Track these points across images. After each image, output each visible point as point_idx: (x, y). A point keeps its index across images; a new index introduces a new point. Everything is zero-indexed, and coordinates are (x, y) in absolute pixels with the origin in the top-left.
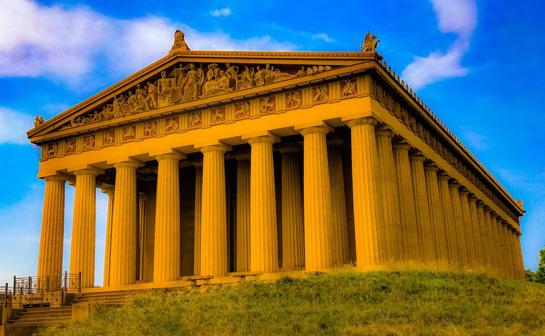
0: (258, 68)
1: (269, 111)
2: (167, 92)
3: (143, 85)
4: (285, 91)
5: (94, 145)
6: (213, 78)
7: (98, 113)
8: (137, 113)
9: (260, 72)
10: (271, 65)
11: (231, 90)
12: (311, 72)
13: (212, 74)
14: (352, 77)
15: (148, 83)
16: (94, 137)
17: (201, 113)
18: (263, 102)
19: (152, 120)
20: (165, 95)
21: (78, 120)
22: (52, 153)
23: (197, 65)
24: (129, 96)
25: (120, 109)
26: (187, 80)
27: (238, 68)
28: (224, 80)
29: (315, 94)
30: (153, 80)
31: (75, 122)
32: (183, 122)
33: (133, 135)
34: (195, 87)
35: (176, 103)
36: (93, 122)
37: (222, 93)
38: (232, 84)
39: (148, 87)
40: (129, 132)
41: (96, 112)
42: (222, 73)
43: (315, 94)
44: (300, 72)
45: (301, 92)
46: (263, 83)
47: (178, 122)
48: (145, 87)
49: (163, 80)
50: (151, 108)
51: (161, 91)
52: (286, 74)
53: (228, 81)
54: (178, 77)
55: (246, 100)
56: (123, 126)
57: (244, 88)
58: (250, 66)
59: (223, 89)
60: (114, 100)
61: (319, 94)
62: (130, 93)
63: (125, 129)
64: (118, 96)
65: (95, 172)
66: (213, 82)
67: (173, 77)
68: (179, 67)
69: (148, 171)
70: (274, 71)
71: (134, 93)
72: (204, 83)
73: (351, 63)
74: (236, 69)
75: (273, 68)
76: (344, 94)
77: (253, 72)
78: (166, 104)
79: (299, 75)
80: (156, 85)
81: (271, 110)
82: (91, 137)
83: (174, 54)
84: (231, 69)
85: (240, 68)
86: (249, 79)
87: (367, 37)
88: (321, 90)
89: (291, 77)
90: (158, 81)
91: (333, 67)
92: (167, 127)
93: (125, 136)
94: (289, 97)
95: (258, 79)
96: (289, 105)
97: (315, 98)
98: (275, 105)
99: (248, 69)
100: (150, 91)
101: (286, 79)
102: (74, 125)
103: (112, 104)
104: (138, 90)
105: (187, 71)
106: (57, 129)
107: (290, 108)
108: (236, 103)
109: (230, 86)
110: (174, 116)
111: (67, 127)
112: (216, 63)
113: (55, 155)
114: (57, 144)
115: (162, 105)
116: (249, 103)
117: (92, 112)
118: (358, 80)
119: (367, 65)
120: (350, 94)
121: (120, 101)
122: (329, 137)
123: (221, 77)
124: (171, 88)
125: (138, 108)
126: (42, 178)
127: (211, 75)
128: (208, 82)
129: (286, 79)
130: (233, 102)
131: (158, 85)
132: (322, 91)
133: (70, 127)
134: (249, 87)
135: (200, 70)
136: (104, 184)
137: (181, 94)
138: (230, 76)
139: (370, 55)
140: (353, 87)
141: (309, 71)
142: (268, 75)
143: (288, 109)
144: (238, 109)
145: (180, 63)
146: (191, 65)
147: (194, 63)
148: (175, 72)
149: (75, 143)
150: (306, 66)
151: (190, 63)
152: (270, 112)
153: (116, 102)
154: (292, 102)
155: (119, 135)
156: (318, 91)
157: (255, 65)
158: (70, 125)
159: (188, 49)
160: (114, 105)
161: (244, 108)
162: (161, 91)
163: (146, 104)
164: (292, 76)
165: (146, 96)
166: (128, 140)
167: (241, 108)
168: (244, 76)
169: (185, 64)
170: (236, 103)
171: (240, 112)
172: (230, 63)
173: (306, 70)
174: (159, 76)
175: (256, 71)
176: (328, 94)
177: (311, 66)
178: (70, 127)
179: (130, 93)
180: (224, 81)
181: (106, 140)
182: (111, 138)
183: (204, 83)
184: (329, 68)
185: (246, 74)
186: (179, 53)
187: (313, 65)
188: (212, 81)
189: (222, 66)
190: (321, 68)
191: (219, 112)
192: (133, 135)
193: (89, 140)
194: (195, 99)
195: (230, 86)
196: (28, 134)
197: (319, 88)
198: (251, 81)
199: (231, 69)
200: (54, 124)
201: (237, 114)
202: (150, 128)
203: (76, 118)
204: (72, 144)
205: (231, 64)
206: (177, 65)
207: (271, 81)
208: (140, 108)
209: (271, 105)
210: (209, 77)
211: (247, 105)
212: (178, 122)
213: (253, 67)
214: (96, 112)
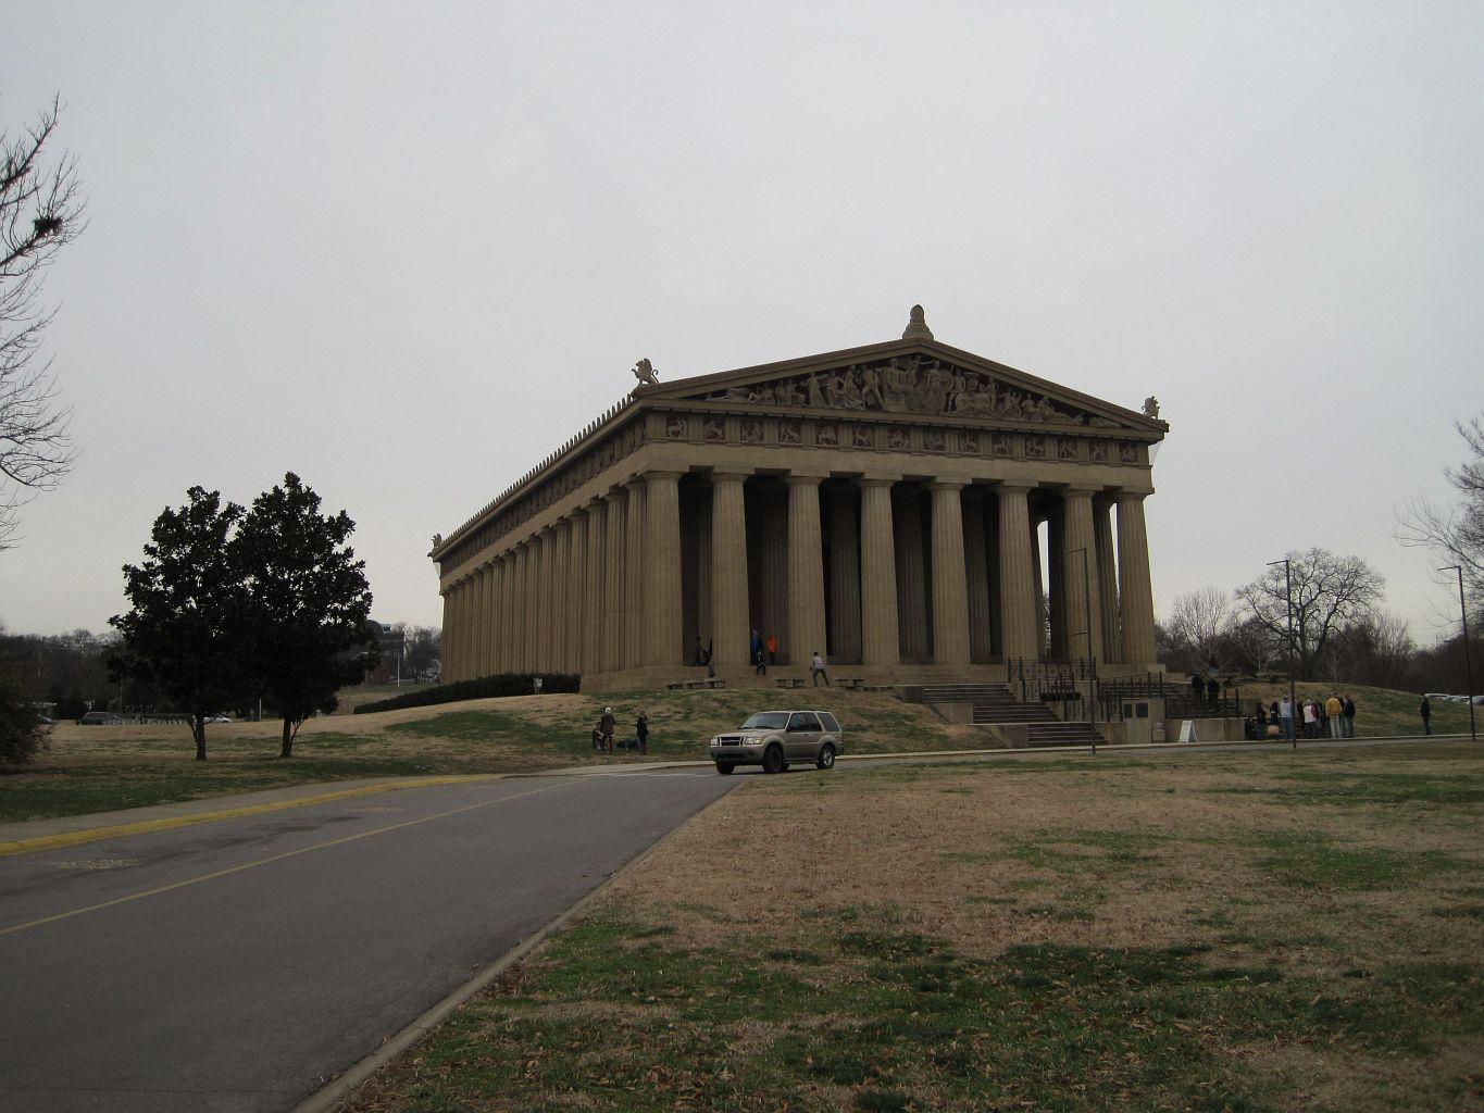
0: (1029, 396)
1: (1038, 456)
4: (1062, 438)
5: (761, 438)
8: (857, 410)
10: (1050, 399)
16: (761, 423)
23: (944, 366)
28: (984, 399)
32: (917, 439)
33: (835, 439)
37: (986, 416)
40: (830, 434)
44: (1078, 419)
47: (909, 438)
48: (858, 371)
49: (893, 369)
55: (1014, 434)
56: (822, 423)
64: (818, 374)
67: (905, 370)
73: (1140, 427)
82: (757, 426)
83: (918, 339)
84: (992, 386)
85: (1003, 387)
91: (1124, 426)
93: (821, 437)
97: (1094, 455)
104: (850, 373)
106: (702, 397)
108: (997, 435)
113: (680, 438)
117: (762, 385)
144: (996, 441)
145: (919, 353)
147: (942, 362)
149: (724, 426)
150: (1094, 415)
155: (808, 434)
166: (825, 445)
169: (925, 358)
170: (997, 435)
174: (885, 363)
176: (1106, 452)
177: (1098, 416)
182: (796, 435)
189: (984, 380)
191: (970, 440)
199: (992, 386)
205: (995, 380)
206: (913, 356)
209: (1039, 448)
210: (959, 385)
212: (909, 438)
213: (1023, 394)
214: (766, 386)
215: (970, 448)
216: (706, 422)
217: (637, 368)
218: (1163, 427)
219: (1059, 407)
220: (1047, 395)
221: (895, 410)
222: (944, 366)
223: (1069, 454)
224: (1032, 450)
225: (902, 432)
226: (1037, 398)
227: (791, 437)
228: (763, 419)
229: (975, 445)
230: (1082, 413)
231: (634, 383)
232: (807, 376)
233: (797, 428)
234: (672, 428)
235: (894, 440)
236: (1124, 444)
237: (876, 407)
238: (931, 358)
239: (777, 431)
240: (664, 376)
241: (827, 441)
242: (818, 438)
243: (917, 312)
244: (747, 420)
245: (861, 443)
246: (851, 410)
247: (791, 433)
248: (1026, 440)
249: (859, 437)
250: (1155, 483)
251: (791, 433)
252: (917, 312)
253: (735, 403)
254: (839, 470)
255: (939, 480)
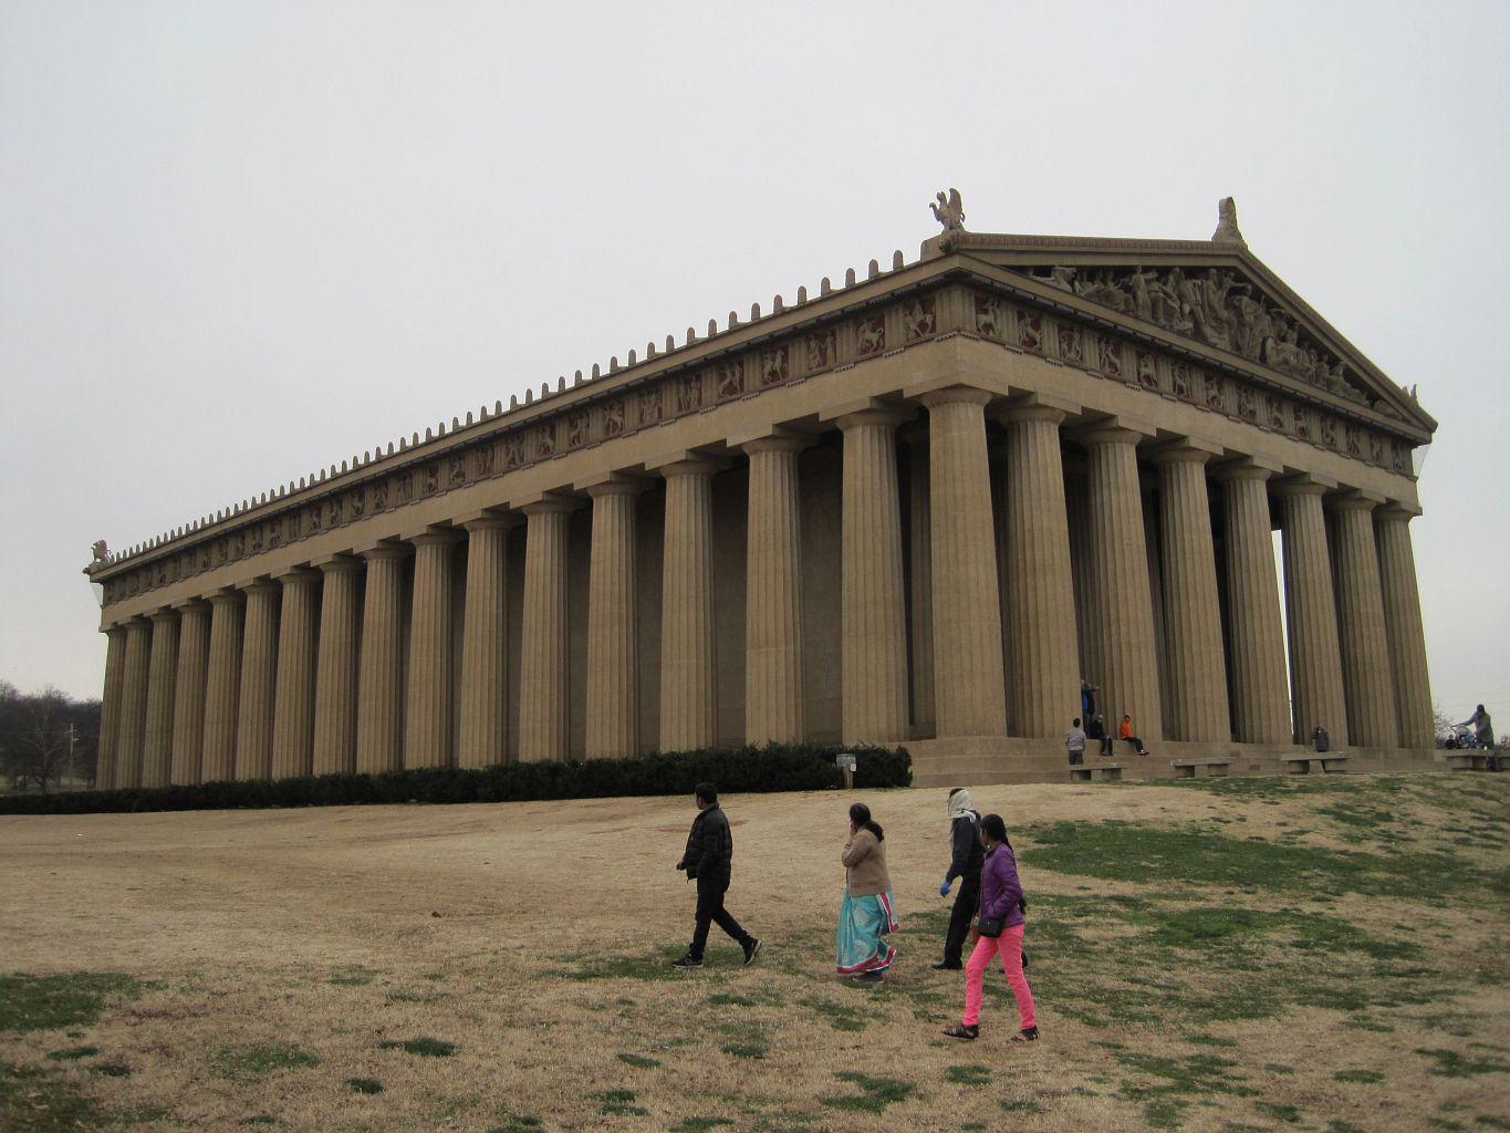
20: (1225, 325)
22: (988, 327)
23: (1257, 296)
37: (1299, 377)
60: (1135, 272)
64: (1146, 269)
73: (1414, 421)
91: (1405, 420)
158: (1053, 278)
169: (1240, 277)
170: (1303, 405)
177: (1385, 401)
193: (1071, 339)
213: (1322, 351)
217: (938, 204)
218: (1429, 426)
219: (1350, 376)
221: (1217, 348)
222: (1257, 296)
226: (1334, 362)
227: (1112, 365)
231: (938, 229)
232: (1130, 271)
234: (984, 319)
237: (1198, 335)
238: (1248, 281)
240: (976, 222)
242: (1139, 374)
243: (1228, 208)
244: (1072, 324)
245: (1181, 390)
247: (1113, 359)
248: (1322, 420)
250: (1423, 501)
251: (1113, 359)
252: (1228, 208)
255: (1257, 462)
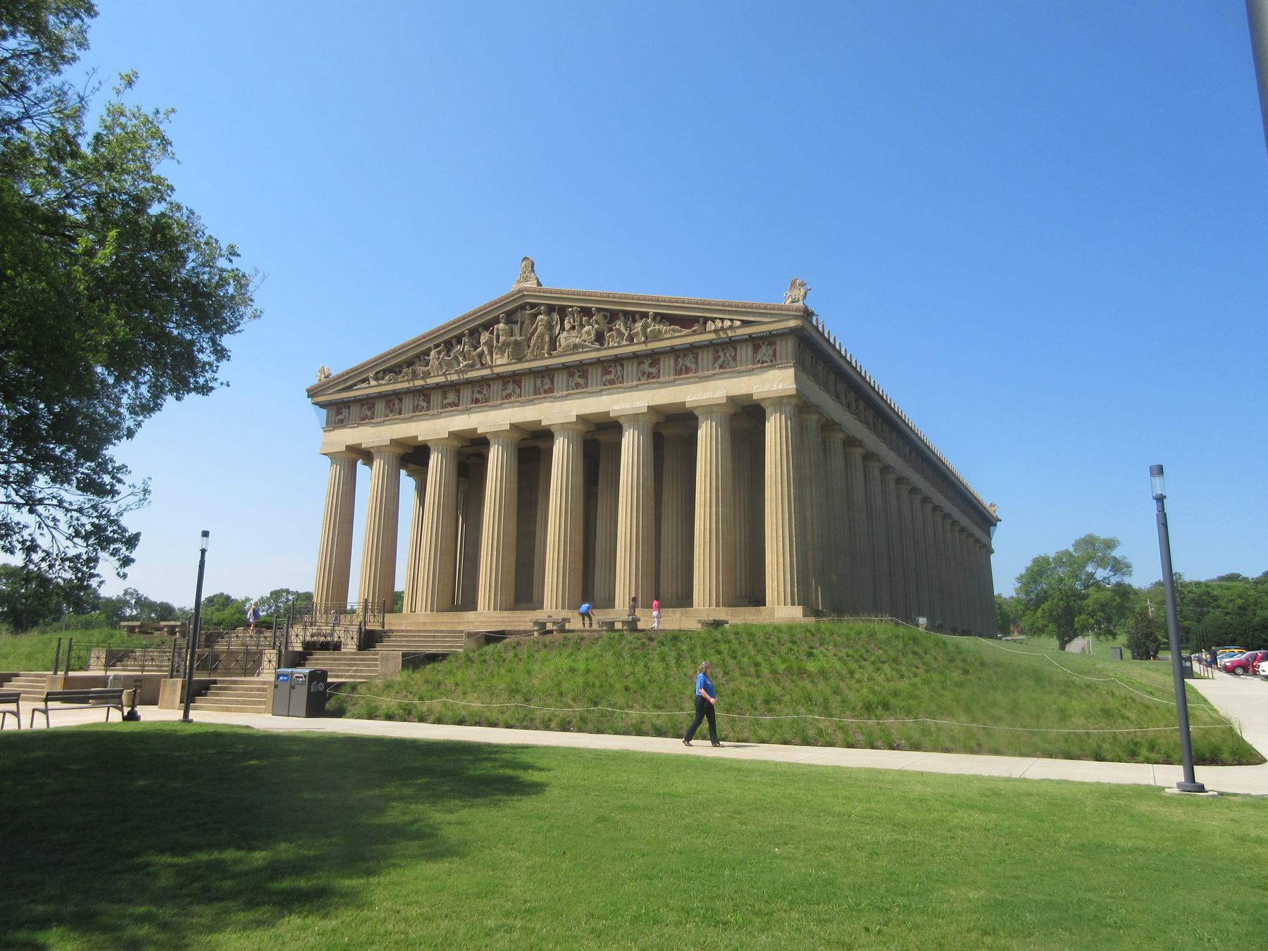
0: (637, 316)
2: (506, 345)
3: (474, 333)
4: (674, 352)
6: (573, 328)
7: (408, 367)
9: (639, 325)
10: (656, 314)
11: (597, 345)
12: (713, 327)
13: (572, 321)
14: (770, 339)
15: (480, 329)
16: (401, 400)
17: (553, 376)
18: (643, 365)
19: (483, 382)
21: (380, 375)
23: (550, 309)
24: (452, 346)
25: (440, 363)
26: (536, 329)
27: (608, 315)
29: (716, 359)
30: (487, 326)
31: (376, 379)
34: (547, 339)
35: (520, 360)
36: (400, 380)
38: (600, 338)
39: (480, 335)
40: (451, 397)
41: (404, 366)
42: (586, 321)
43: (716, 359)
45: (697, 354)
46: (643, 339)
47: (520, 387)
49: (501, 326)
50: (483, 366)
51: (498, 341)
52: (677, 327)
53: (593, 333)
54: (523, 323)
55: (619, 360)
57: (616, 345)
58: (626, 313)
59: (587, 343)
61: (722, 358)
62: (454, 342)
63: (445, 393)
64: (437, 346)
65: (399, 451)
66: (574, 333)
67: (516, 322)
68: (526, 310)
69: (474, 450)
70: (660, 322)
71: (459, 342)
72: (559, 334)
74: (605, 317)
75: (658, 318)
76: (758, 362)
77: (629, 323)
78: (505, 361)
79: (694, 331)
80: (492, 333)
81: (654, 378)
82: (396, 402)
83: (520, 291)
85: (612, 316)
86: (624, 331)
87: (793, 285)
88: (725, 354)
89: (683, 333)
90: (496, 326)
92: (504, 393)
94: (680, 360)
95: (637, 334)
96: (679, 372)
98: (659, 371)
99: (622, 318)
100: (482, 340)
101: (677, 334)
102: (373, 383)
103: (429, 355)
105: (535, 315)
106: (350, 388)
107: (681, 377)
109: (596, 340)
110: (514, 379)
111: (364, 385)
112: (579, 307)
114: (349, 408)
115: (499, 362)
116: (622, 366)
118: (778, 344)
119: (792, 323)
120: (767, 362)
121: (439, 353)
122: (733, 418)
123: (584, 326)
124: (513, 339)
125: (465, 363)
126: (326, 454)
127: (570, 322)
128: (565, 333)
129: (677, 334)
130: (598, 362)
131: (495, 333)
132: (728, 355)
133: (367, 385)
134: (624, 343)
135: (556, 316)
136: (410, 465)
137: (526, 348)
138: (596, 326)
139: (797, 310)
140: (771, 352)
141: (710, 326)
142: (652, 328)
143: (677, 377)
144: (606, 372)
146: (542, 308)
148: (518, 316)
150: (706, 320)
151: (541, 304)
152: (652, 380)
153: (432, 353)
154: (684, 368)
156: (721, 354)
157: (633, 314)
159: (539, 284)
160: (431, 357)
161: (615, 371)
162: (498, 341)
163: (477, 359)
164: (685, 331)
165: (476, 348)
167: (610, 373)
168: (617, 327)
169: (533, 306)
171: (608, 377)
172: (597, 308)
173: (705, 323)
175: (634, 321)
177: (713, 320)
178: (367, 385)
179: (454, 342)
180: (588, 333)
181: (417, 406)
182: (424, 404)
183: (559, 334)
184: (738, 323)
185: (619, 325)
186: (526, 289)
187: (716, 318)
188: (571, 332)
189: (586, 312)
190: (727, 323)
191: (580, 376)
192: (457, 401)
193: (394, 405)
194: (546, 355)
195: (596, 340)
196: (308, 391)
197: (723, 350)
198: (627, 334)
200: (345, 380)
201: (604, 379)
202: (480, 392)
203: (377, 373)
204: (369, 409)
205: (599, 310)
206: (523, 307)
207: (657, 336)
208: (468, 365)
209: (654, 370)
210: (567, 326)
211: (619, 368)
213: (631, 317)
214: (404, 366)
215: (578, 386)
216: (363, 405)
220: (652, 311)
221: (502, 363)
223: (688, 370)
224: (644, 373)
225: (514, 382)
228: (398, 395)
229: (581, 381)
230: (701, 321)
233: (427, 398)
235: (504, 393)
236: (756, 342)
239: (411, 402)
241: (450, 405)
246: (462, 372)
249: (476, 395)
253: (373, 388)
254: (456, 429)
